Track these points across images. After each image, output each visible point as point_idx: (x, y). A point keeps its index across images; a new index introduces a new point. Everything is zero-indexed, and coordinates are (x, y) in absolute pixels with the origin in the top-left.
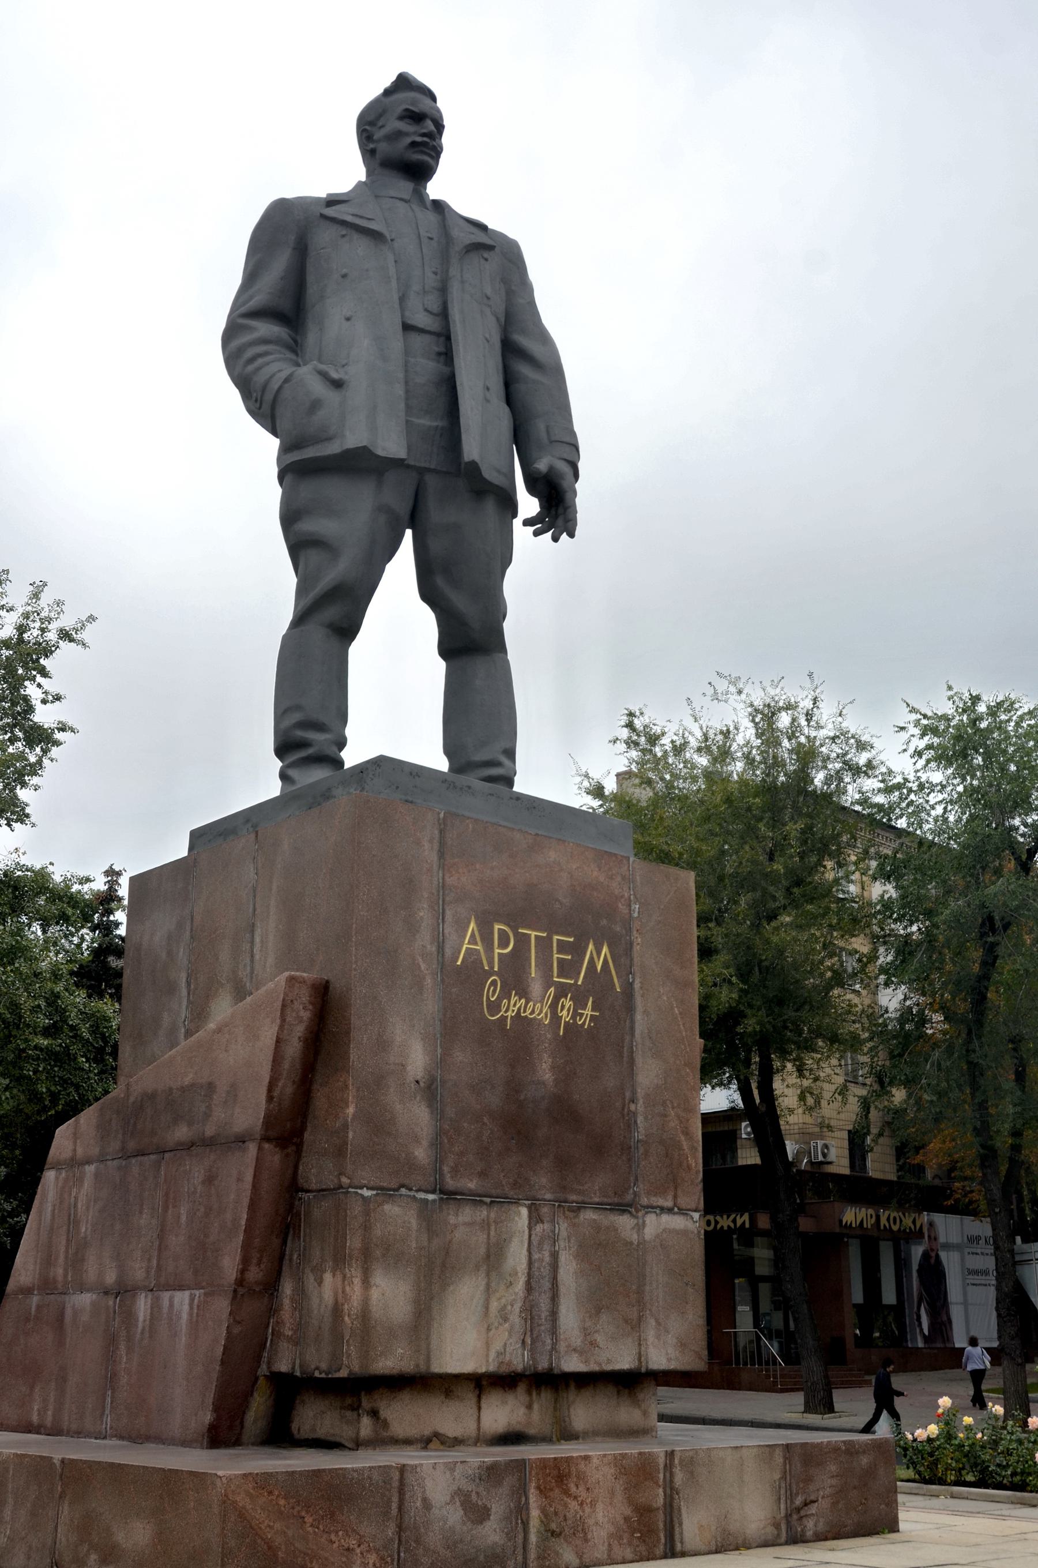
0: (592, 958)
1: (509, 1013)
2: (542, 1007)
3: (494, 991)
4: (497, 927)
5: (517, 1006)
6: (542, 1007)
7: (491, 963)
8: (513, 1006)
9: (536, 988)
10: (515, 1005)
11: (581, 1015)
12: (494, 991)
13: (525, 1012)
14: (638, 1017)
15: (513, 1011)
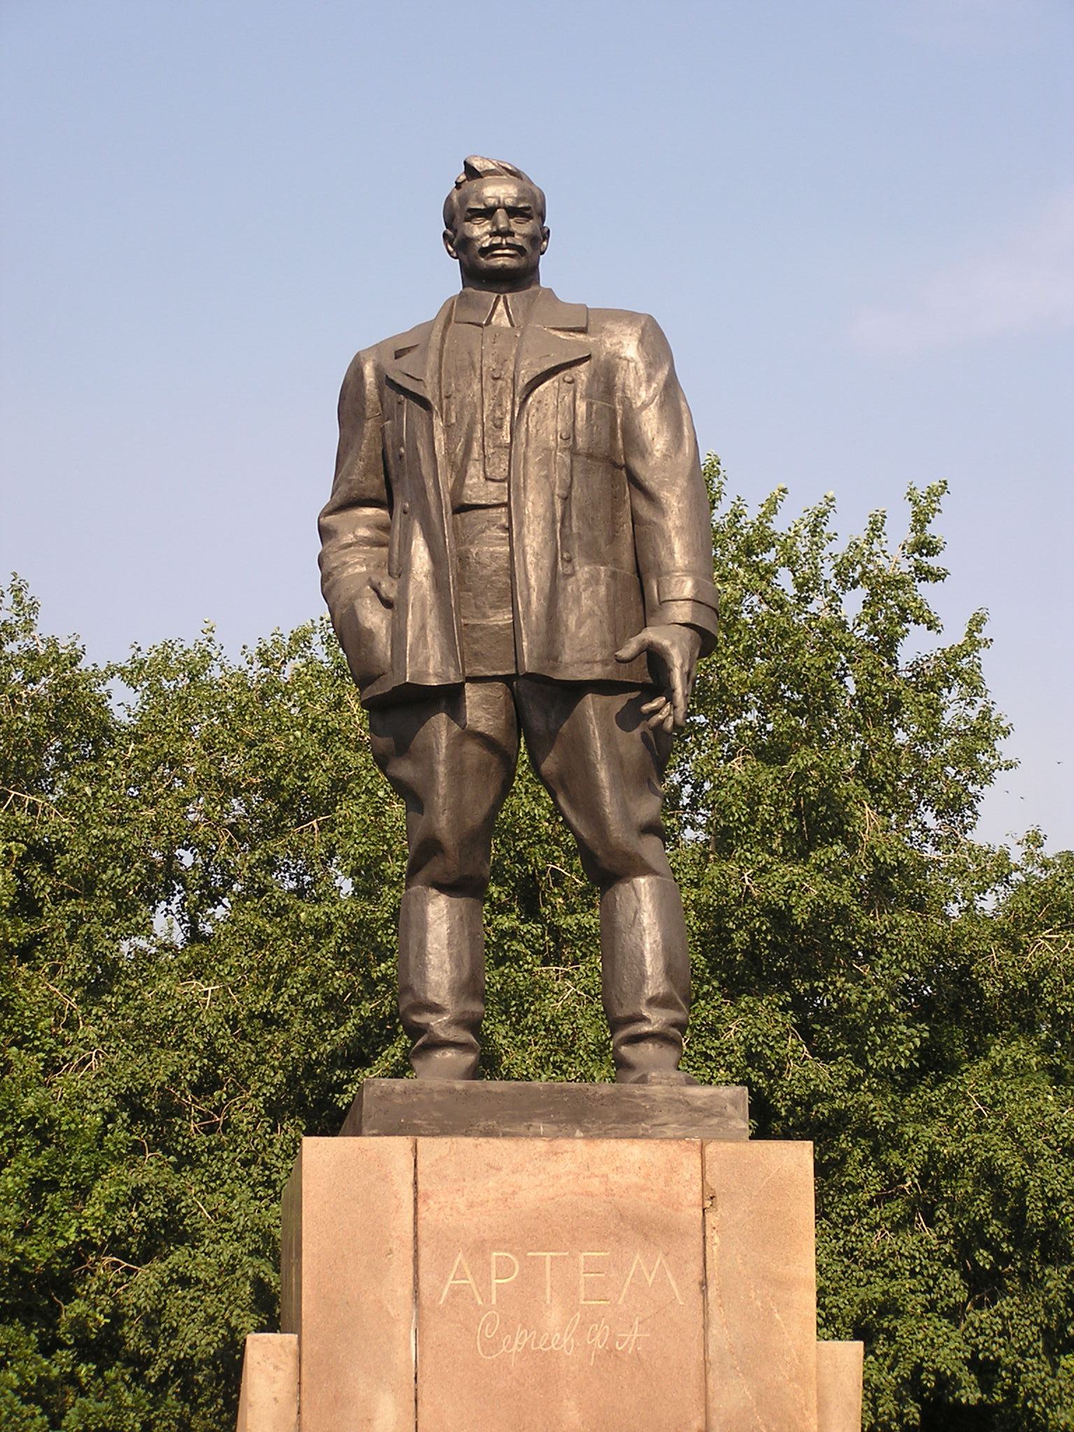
0: (639, 1271)
1: (513, 1350)
2: (562, 1336)
3: (492, 1328)
4: (495, 1254)
5: (526, 1339)
6: (562, 1336)
7: (486, 1298)
8: (521, 1338)
9: (554, 1317)
10: (521, 1340)
11: (622, 1341)
12: (492, 1328)
13: (536, 1345)
14: (714, 1331)
15: (519, 1346)
